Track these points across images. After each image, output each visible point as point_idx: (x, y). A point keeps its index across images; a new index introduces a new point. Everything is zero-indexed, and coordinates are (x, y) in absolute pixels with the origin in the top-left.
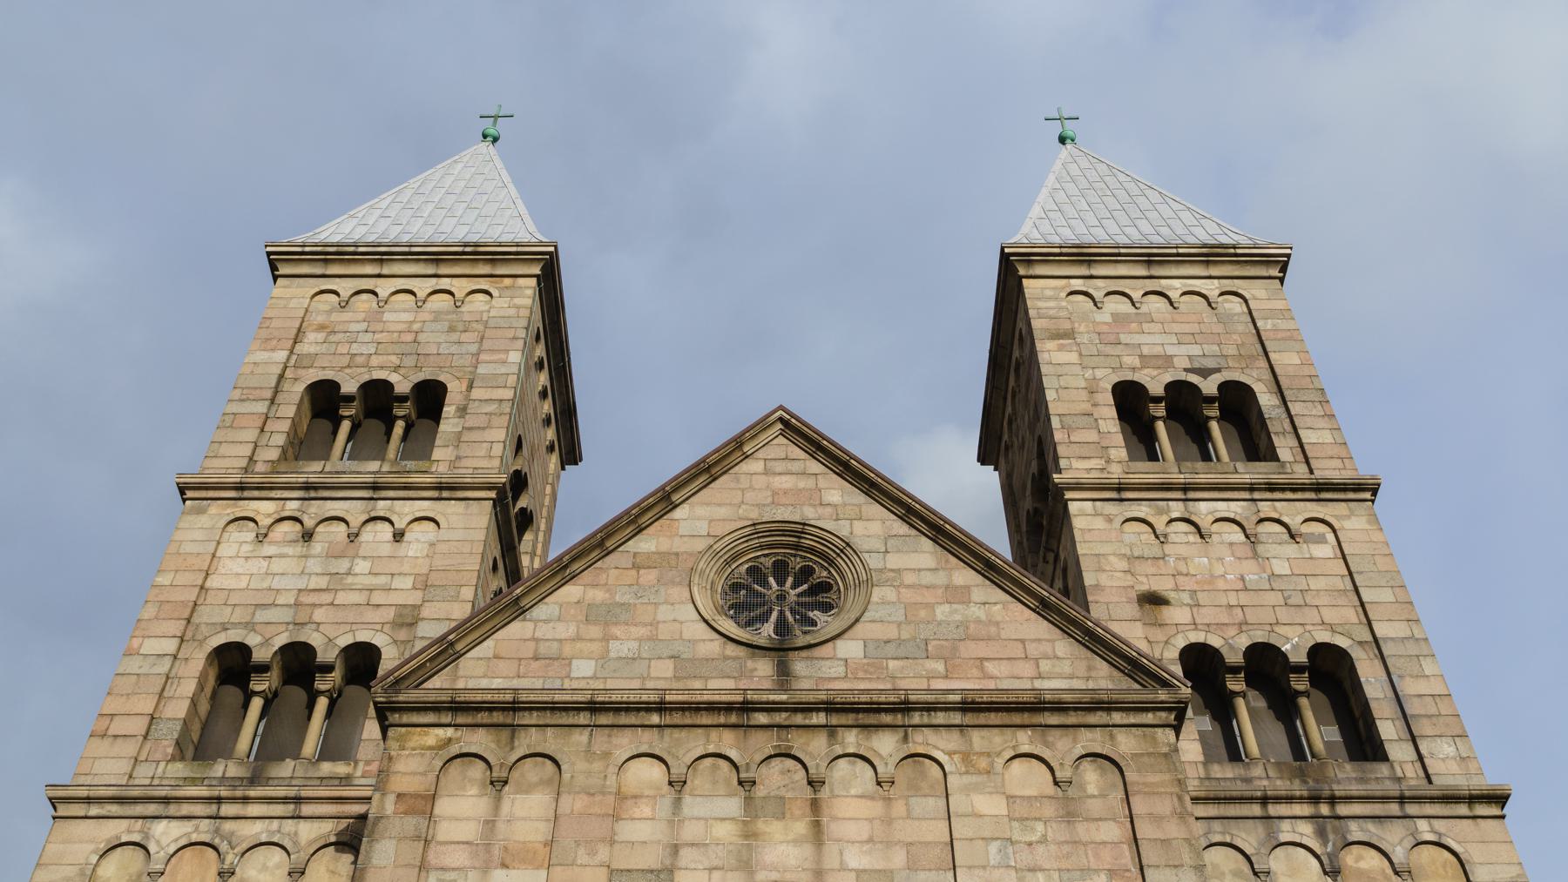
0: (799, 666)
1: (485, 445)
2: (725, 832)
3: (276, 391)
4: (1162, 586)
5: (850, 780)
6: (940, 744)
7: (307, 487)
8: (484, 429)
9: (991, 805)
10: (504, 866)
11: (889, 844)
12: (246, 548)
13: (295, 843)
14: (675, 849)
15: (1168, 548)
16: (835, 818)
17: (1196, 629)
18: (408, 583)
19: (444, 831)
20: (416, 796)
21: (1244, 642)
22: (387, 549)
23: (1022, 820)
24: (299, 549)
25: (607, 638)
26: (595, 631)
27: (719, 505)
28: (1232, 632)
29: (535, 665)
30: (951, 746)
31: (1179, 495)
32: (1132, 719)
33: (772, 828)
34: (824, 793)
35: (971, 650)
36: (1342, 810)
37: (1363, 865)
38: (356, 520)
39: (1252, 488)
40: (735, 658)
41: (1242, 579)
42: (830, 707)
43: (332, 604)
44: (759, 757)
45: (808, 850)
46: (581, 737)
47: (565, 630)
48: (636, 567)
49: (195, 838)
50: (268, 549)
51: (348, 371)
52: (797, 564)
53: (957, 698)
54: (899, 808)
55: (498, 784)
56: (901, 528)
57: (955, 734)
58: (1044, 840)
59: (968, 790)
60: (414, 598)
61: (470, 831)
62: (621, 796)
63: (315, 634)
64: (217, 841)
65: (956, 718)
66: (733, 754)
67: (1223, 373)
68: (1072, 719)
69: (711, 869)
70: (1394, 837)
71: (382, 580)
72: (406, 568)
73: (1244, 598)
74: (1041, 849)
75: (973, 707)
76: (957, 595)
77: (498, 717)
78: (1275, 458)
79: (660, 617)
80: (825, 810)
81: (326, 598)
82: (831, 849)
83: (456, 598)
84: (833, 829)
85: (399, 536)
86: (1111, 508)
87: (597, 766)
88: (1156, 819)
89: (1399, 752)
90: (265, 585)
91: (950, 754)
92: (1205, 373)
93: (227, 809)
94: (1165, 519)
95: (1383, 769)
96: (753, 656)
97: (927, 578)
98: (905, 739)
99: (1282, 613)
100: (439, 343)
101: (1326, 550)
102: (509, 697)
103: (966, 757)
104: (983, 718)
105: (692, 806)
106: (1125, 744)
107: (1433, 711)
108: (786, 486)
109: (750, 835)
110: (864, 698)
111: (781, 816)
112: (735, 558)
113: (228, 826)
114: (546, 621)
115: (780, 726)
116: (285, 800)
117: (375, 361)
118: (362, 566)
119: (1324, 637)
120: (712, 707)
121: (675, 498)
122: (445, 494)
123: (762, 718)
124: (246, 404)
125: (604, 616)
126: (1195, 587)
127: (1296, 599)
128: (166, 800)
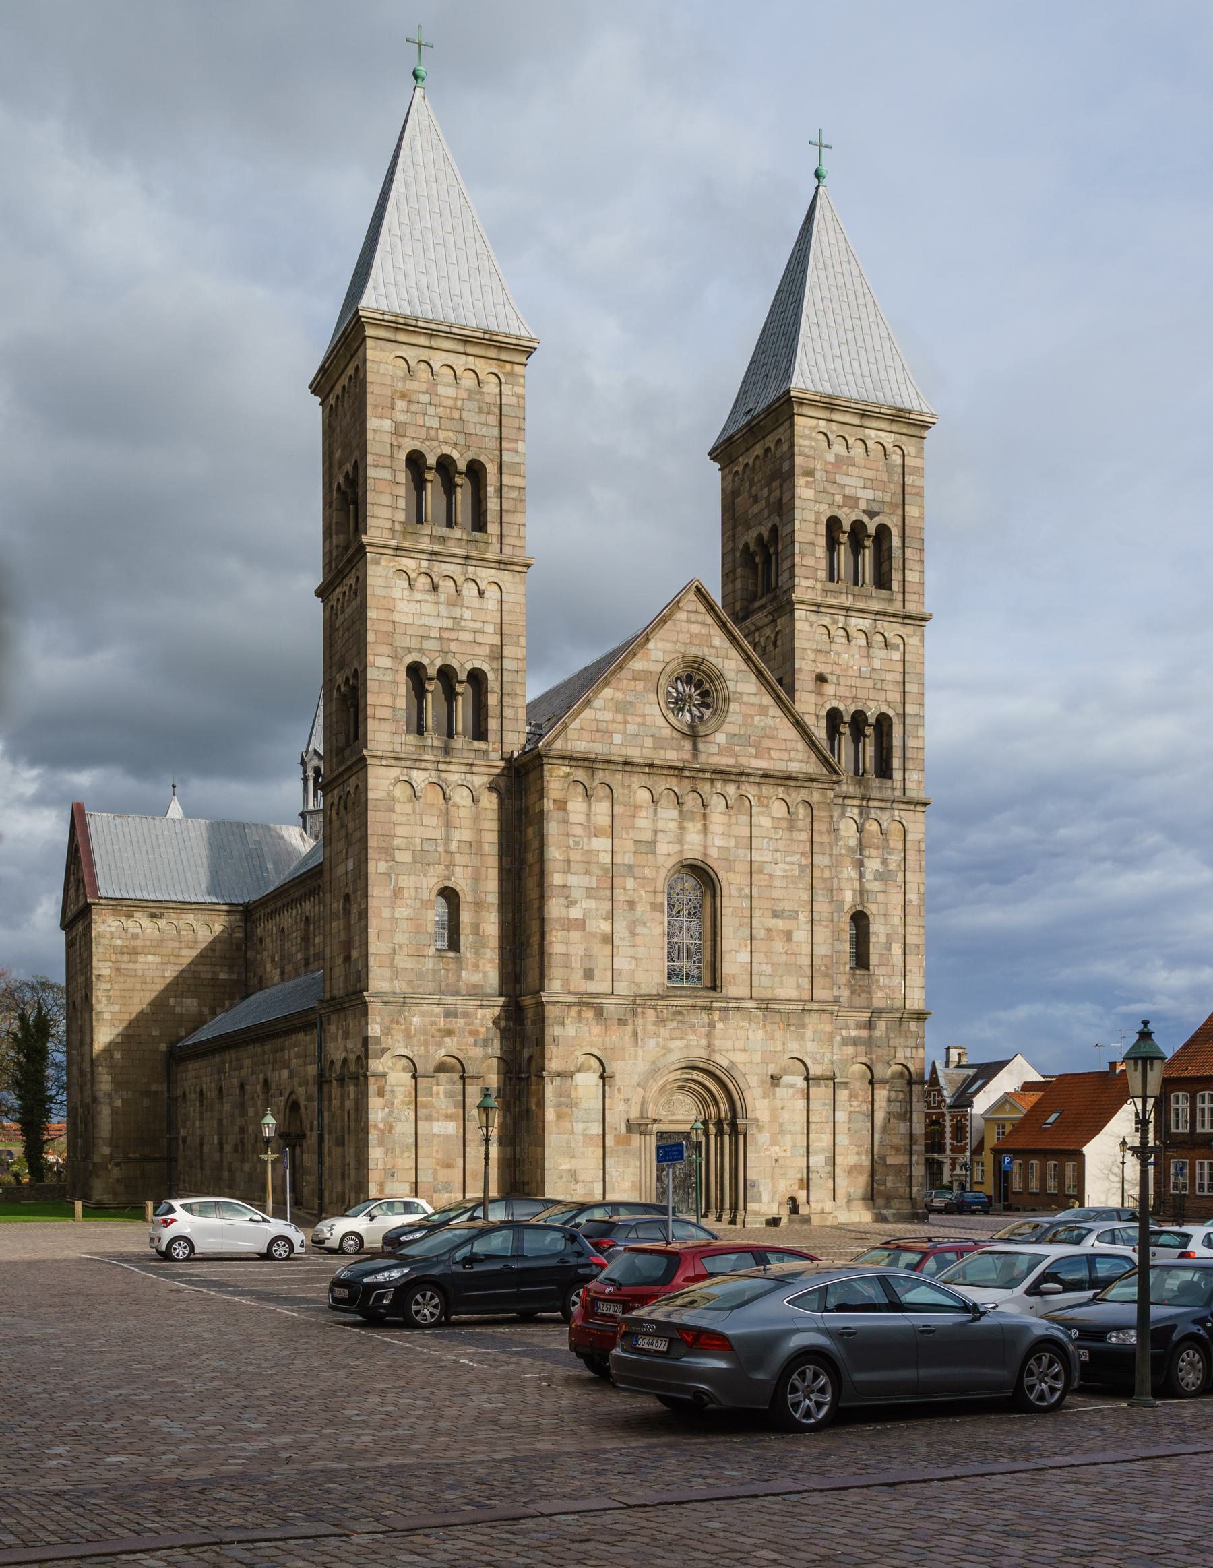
0: (701, 746)
2: (673, 826)
4: (826, 670)
5: (717, 804)
6: (751, 791)
9: (766, 822)
10: (596, 836)
11: (729, 836)
12: (406, 593)
13: (474, 786)
14: (656, 832)
16: (711, 823)
18: (490, 628)
19: (574, 818)
20: (560, 801)
21: (852, 709)
22: (476, 602)
23: (775, 828)
25: (626, 722)
26: (620, 718)
27: (668, 641)
28: (849, 702)
29: (598, 735)
30: (754, 793)
31: (844, 613)
32: (820, 786)
33: (689, 825)
34: (708, 811)
35: (767, 743)
36: (871, 804)
37: (871, 828)
38: (460, 579)
39: (876, 613)
40: (676, 739)
42: (714, 771)
43: (457, 640)
44: (685, 792)
45: (702, 836)
46: (619, 776)
47: (608, 716)
48: (634, 679)
49: (431, 780)
50: (418, 596)
51: (427, 443)
52: (696, 677)
53: (761, 772)
54: (734, 818)
55: (588, 796)
56: (743, 666)
57: (757, 787)
58: (781, 839)
59: (759, 814)
61: (581, 818)
62: (636, 807)
63: (454, 660)
64: (441, 783)
65: (758, 780)
66: (676, 790)
68: (799, 784)
69: (669, 843)
70: (885, 817)
71: (478, 625)
72: (489, 618)
73: (858, 682)
74: (780, 842)
75: (767, 777)
76: (763, 710)
77: (586, 764)
78: (890, 589)
79: (646, 712)
80: (708, 819)
81: (453, 635)
82: (710, 836)
84: (713, 828)
86: (813, 617)
87: (626, 791)
88: (821, 833)
89: (897, 775)
90: (422, 622)
91: (754, 796)
92: (871, 514)
93: (441, 767)
94: (835, 627)
95: (889, 783)
96: (683, 738)
97: (753, 699)
98: (738, 787)
99: (872, 694)
101: (897, 656)
102: (594, 756)
103: (759, 798)
104: (767, 780)
105: (662, 813)
106: (816, 797)
108: (696, 631)
109: (682, 828)
110: (728, 769)
111: (692, 820)
113: (444, 775)
114: (600, 710)
115: (694, 777)
116: (466, 764)
117: (442, 435)
119: (884, 709)
120: (670, 768)
122: (502, 566)
123: (687, 773)
124: (378, 469)
125: (623, 708)
126: (839, 672)
127: (878, 686)
128: (416, 760)
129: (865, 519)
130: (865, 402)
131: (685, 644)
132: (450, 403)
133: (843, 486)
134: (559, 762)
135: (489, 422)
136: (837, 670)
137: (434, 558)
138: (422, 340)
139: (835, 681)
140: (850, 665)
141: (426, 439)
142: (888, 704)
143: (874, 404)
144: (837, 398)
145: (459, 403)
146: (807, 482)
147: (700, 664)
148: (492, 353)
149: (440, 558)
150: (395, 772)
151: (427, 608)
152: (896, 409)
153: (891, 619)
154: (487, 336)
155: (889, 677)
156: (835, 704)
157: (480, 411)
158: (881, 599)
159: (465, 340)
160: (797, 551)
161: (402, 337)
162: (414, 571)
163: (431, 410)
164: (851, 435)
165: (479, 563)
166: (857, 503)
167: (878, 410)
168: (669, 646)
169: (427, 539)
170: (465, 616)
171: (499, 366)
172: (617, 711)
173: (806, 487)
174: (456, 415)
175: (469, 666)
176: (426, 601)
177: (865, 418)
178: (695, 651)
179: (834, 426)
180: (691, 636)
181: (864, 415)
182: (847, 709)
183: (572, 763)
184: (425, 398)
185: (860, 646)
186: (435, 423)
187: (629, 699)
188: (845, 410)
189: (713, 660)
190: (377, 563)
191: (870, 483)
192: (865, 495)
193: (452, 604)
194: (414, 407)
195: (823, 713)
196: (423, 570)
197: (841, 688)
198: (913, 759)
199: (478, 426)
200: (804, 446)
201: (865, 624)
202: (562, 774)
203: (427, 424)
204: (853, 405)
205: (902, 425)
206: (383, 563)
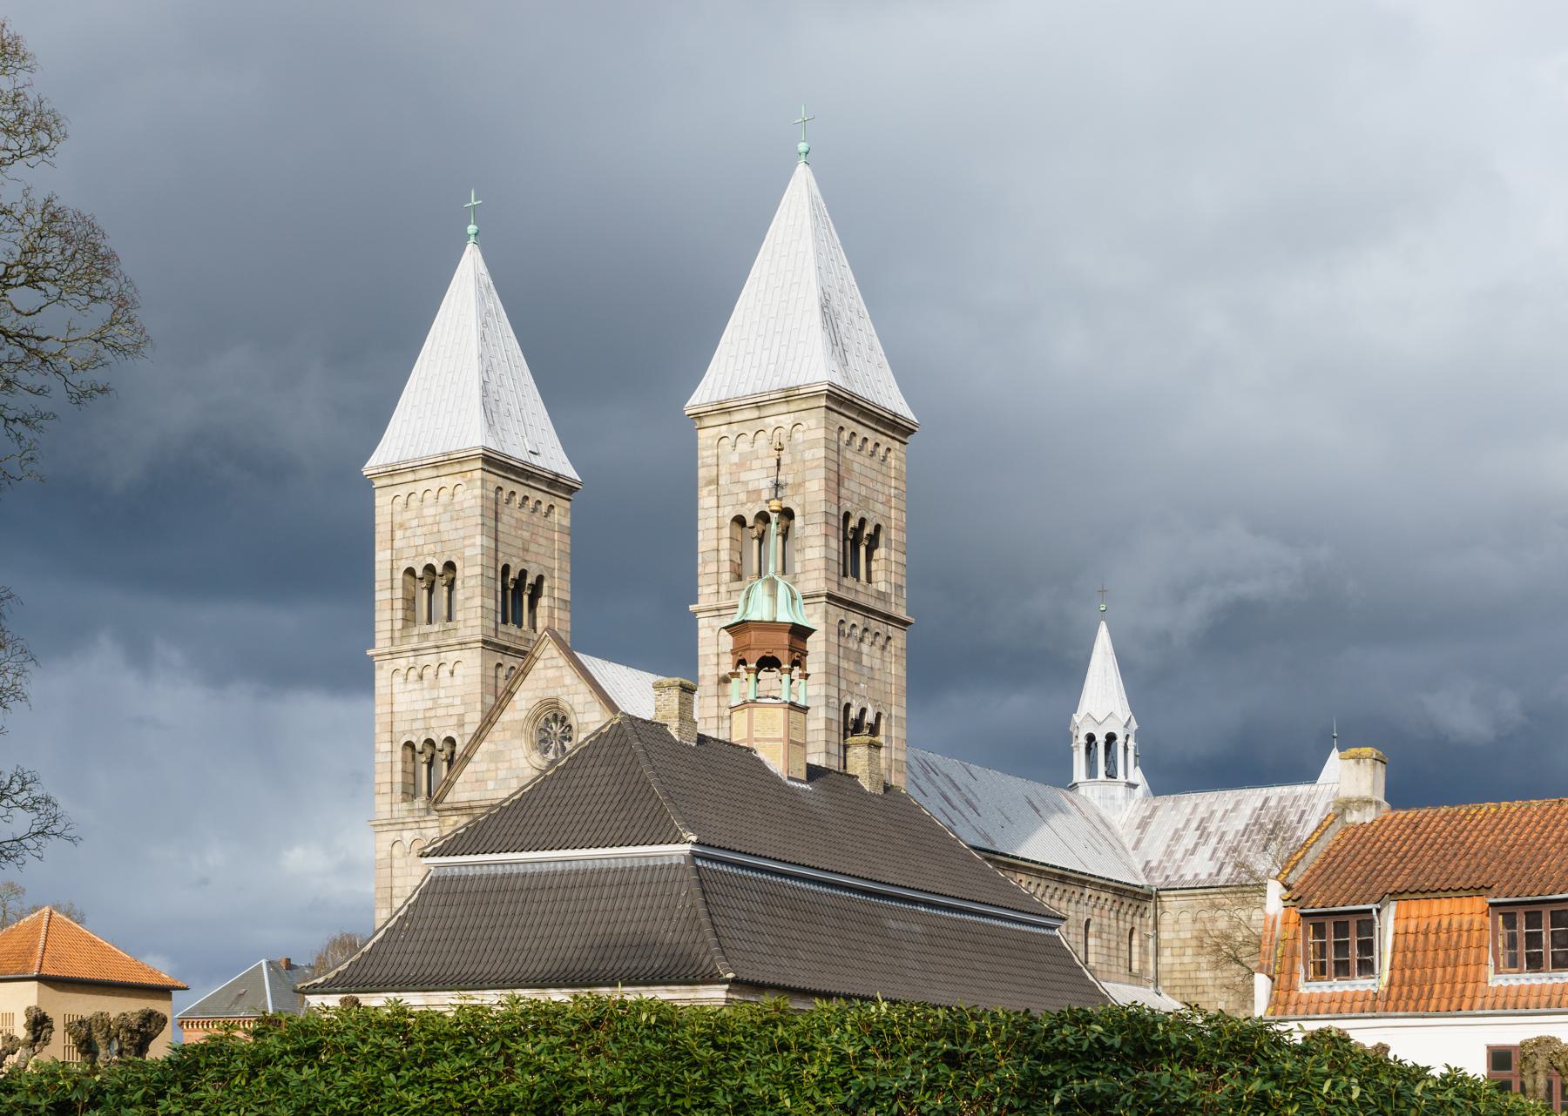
3: (392, 580)
7: (414, 650)
8: (472, 598)
12: (402, 686)
18: (457, 701)
24: (417, 686)
25: (497, 769)
26: (492, 766)
47: (483, 767)
48: (504, 730)
50: (410, 687)
60: (461, 710)
71: (450, 700)
77: (468, 811)
83: (474, 710)
85: (452, 673)
93: (422, 825)
112: (537, 718)
113: (424, 831)
117: (426, 549)
118: (442, 693)
121: (513, 690)
122: (464, 646)
125: (495, 757)
128: (403, 823)
131: (543, 689)
132: (430, 520)
133: (746, 483)
134: (449, 813)
135: (458, 527)
138: (410, 477)
141: (416, 556)
144: (727, 401)
145: (438, 518)
146: (710, 491)
147: (557, 703)
148: (457, 468)
149: (422, 652)
150: (393, 836)
151: (416, 696)
157: (452, 519)
159: (435, 466)
160: (700, 561)
161: (397, 480)
163: (419, 531)
164: (751, 430)
165: (448, 648)
166: (760, 495)
167: (767, 398)
168: (530, 694)
170: (441, 696)
172: (491, 761)
173: (709, 496)
174: (435, 529)
175: (443, 737)
176: (415, 690)
177: (762, 409)
178: (551, 693)
180: (548, 681)
181: (758, 406)
183: (459, 812)
184: (414, 523)
186: (420, 541)
187: (501, 748)
188: (740, 408)
189: (565, 698)
190: (381, 668)
193: (432, 688)
194: (408, 533)
200: (708, 457)
202: (451, 823)
204: (743, 402)
205: (799, 402)
206: (385, 667)
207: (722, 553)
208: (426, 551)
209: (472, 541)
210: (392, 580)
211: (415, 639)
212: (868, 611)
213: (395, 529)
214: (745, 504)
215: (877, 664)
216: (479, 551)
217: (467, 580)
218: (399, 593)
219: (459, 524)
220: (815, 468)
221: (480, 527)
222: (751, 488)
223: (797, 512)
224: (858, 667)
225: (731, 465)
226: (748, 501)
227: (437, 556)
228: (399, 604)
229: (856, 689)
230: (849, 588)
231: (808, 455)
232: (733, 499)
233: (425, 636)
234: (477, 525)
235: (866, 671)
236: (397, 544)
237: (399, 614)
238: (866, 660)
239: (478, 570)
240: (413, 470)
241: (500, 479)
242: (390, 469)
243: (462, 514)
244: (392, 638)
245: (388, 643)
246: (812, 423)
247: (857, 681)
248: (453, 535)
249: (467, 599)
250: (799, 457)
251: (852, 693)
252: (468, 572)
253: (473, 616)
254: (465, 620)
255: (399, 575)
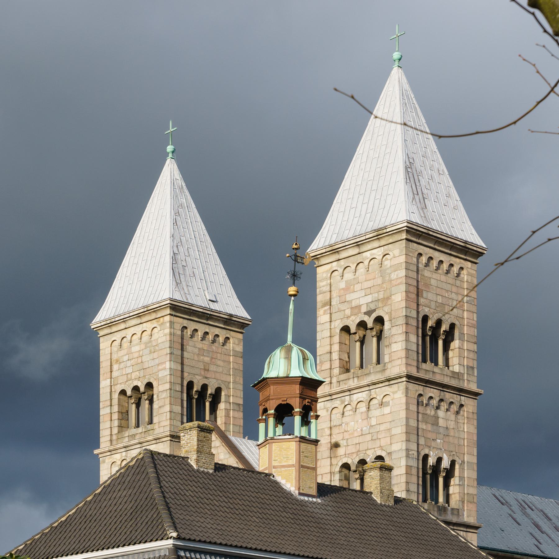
1: (165, 414)
3: (111, 399)
7: (125, 447)
8: (163, 406)
15: (345, 419)
17: (345, 457)
21: (357, 460)
28: (355, 455)
31: (348, 393)
39: (368, 386)
41: (362, 430)
51: (127, 383)
67: (377, 312)
73: (361, 439)
94: (343, 406)
100: (148, 361)
107: (399, 482)
117: (134, 376)
122: (158, 441)
127: (375, 437)
129: (366, 318)
130: (355, 237)
132: (136, 355)
133: (350, 302)
136: (346, 436)
137: (128, 449)
138: (123, 326)
139: (345, 444)
140: (356, 428)
142: (381, 448)
143: (360, 235)
146: (325, 311)
148: (153, 316)
149: (130, 448)
152: (376, 231)
153: (381, 385)
154: (145, 310)
155: (382, 427)
156: (344, 461)
157: (151, 352)
158: (377, 372)
159: (139, 316)
161: (114, 329)
162: (119, 460)
163: (129, 363)
164: (353, 263)
166: (360, 310)
169: (126, 439)
171: (157, 322)
174: (140, 361)
179: (342, 262)
181: (358, 245)
182: (353, 461)
184: (126, 358)
185: (362, 413)
186: (129, 370)
190: (104, 462)
191: (368, 291)
192: (364, 301)
194: (122, 365)
195: (338, 469)
196: (123, 458)
197: (349, 447)
198: (397, 484)
199: (150, 361)
201: (363, 396)
203: (127, 373)
205: (387, 238)
206: (107, 461)
207: (333, 354)
208: (133, 378)
209: (164, 365)
210: (111, 399)
211: (127, 439)
212: (443, 386)
213: (113, 363)
214: (350, 317)
215: (452, 425)
216: (168, 372)
217: (160, 394)
218: (116, 408)
219: (155, 355)
220: (399, 284)
221: (169, 355)
222: (354, 304)
223: (386, 318)
224: (435, 427)
225: (340, 290)
226: (352, 315)
227: (141, 379)
228: (115, 416)
229: (433, 444)
230: (426, 370)
231: (394, 276)
232: (340, 315)
233: (133, 436)
234: (167, 354)
235: (441, 430)
236: (115, 374)
237: (116, 423)
238: (441, 422)
239: (167, 386)
240: (124, 320)
241: (185, 321)
242: (108, 322)
243: (157, 348)
244: (111, 440)
245: (108, 444)
246: (397, 252)
247: (434, 438)
248: (152, 363)
249: (160, 407)
250: (387, 278)
251: (430, 447)
252: (161, 388)
253: (164, 419)
254: (159, 423)
255: (116, 396)
